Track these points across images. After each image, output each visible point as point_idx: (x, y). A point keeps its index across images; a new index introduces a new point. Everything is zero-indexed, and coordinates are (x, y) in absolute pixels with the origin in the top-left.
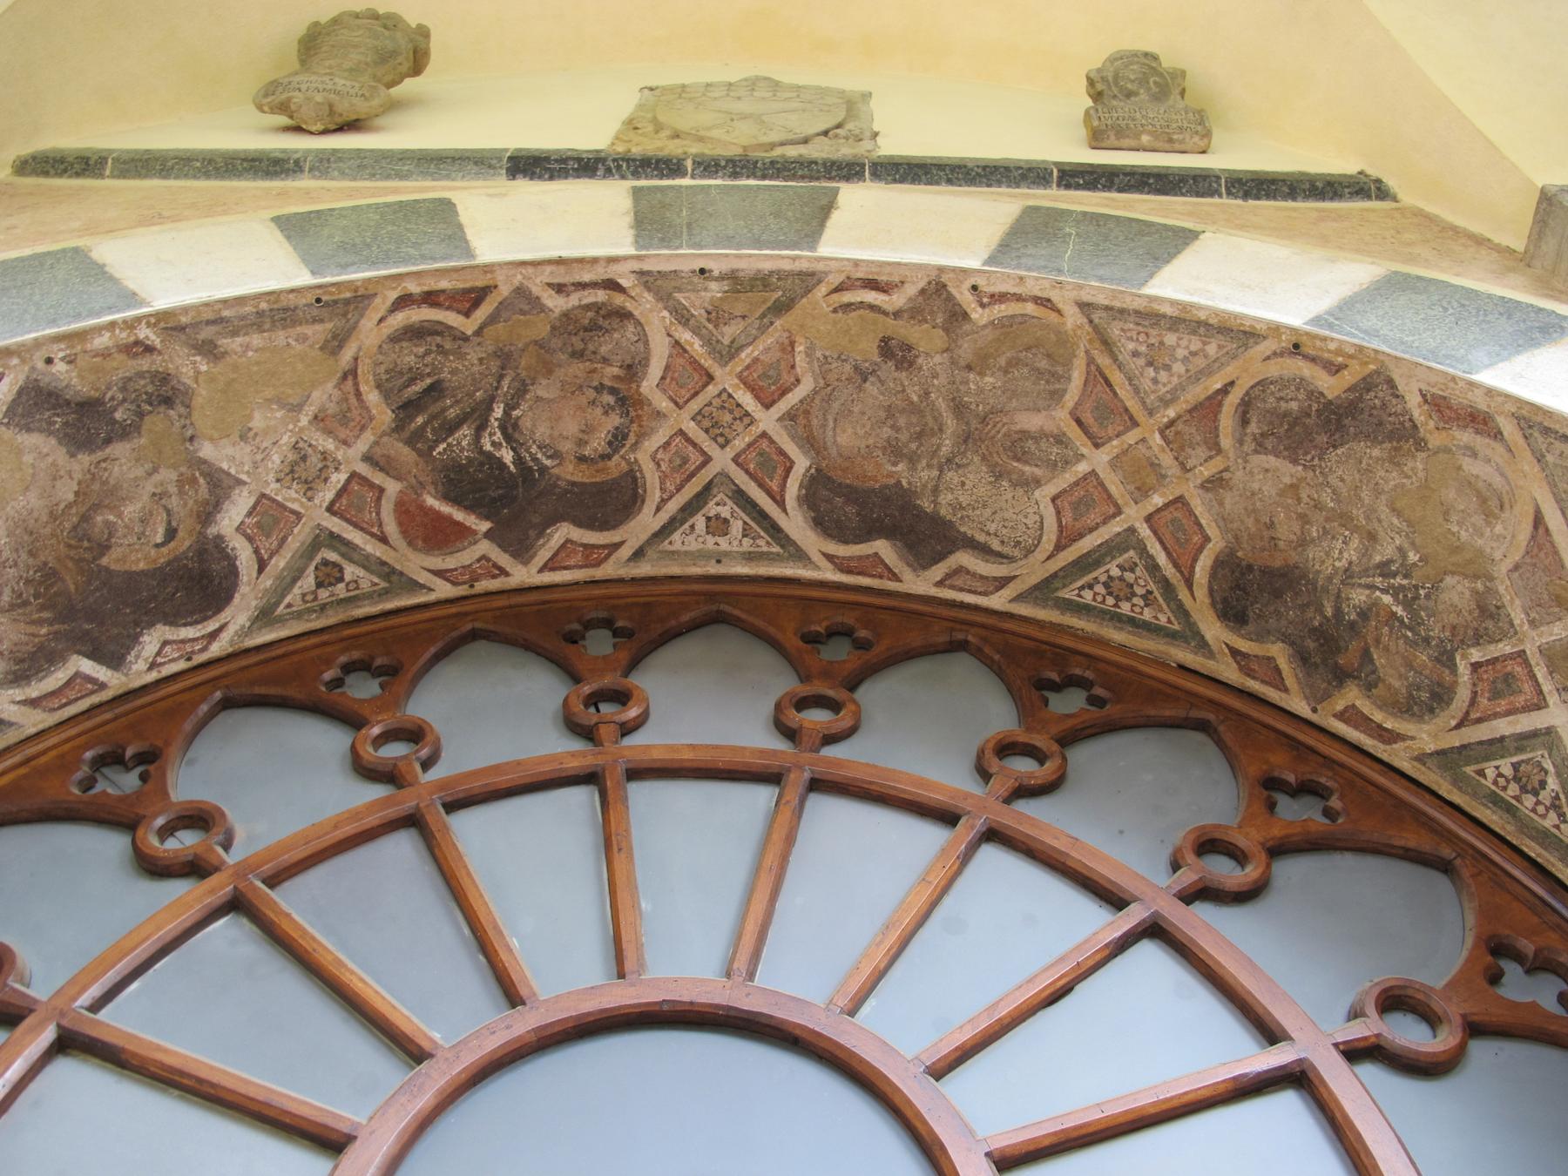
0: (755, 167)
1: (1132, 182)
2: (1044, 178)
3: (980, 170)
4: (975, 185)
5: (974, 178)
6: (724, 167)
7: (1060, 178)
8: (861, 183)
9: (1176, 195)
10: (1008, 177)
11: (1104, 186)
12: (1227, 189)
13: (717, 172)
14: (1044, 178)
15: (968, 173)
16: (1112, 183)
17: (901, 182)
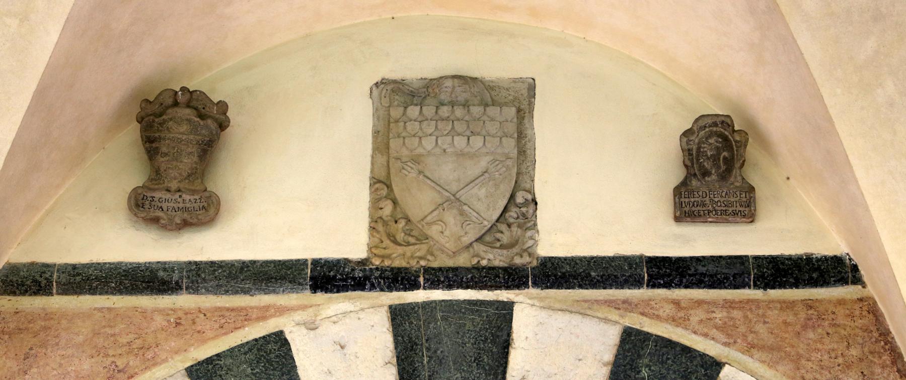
0: (462, 281)
1: (694, 281)
2: (639, 281)
3: (599, 278)
4: (596, 288)
5: (596, 283)
6: (443, 282)
7: (649, 281)
8: (526, 290)
9: (721, 288)
10: (616, 282)
11: (676, 285)
12: (754, 282)
13: (439, 285)
14: (639, 281)
15: (592, 281)
16: (681, 281)
17: (551, 288)
